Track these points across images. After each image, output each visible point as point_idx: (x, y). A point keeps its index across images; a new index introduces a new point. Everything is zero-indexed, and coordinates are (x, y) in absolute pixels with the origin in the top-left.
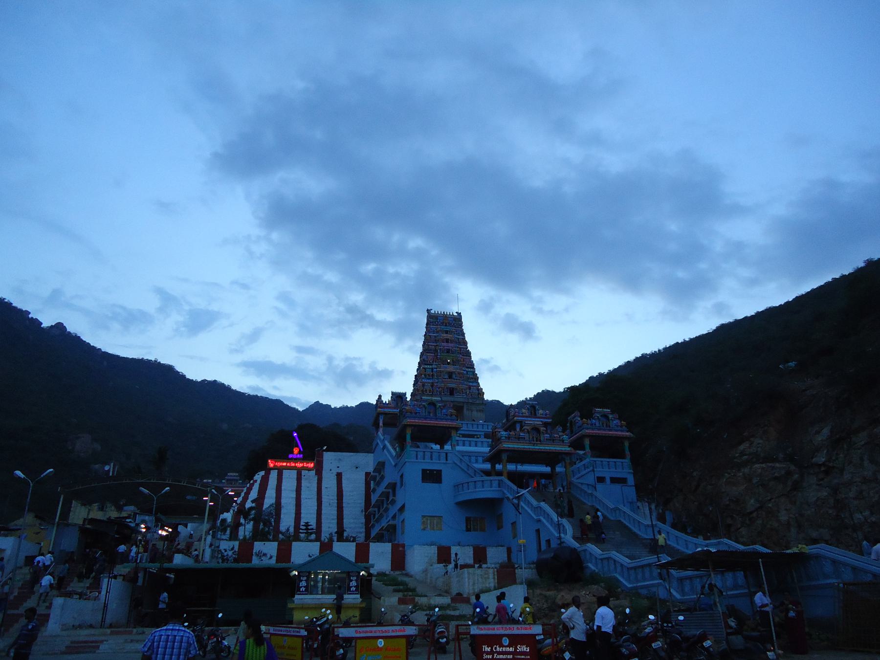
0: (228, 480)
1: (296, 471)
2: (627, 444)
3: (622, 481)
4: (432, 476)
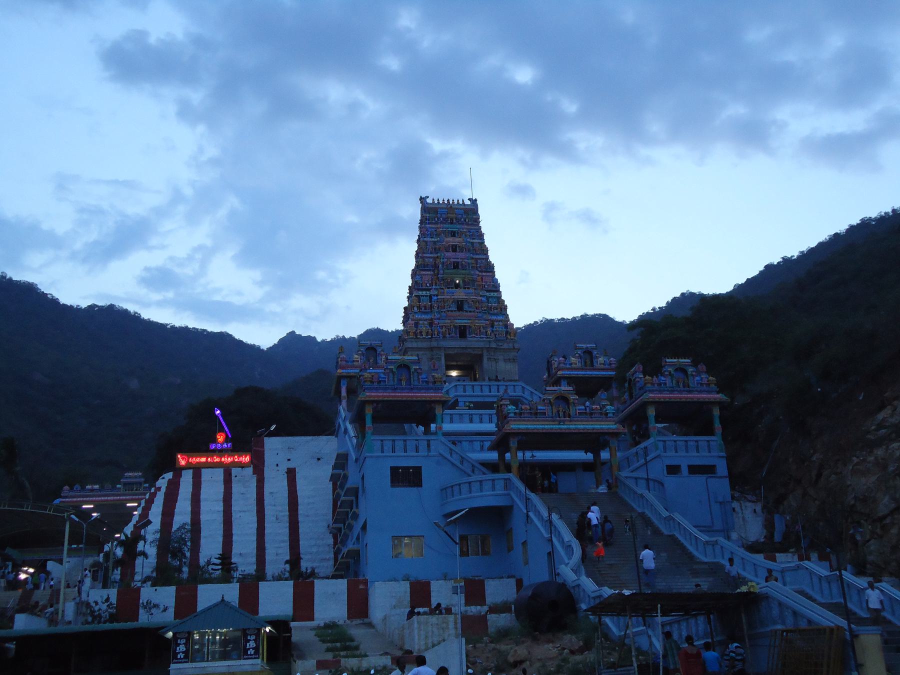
0: (125, 484)
1: (222, 470)
2: (716, 412)
3: (708, 470)
4: (405, 477)
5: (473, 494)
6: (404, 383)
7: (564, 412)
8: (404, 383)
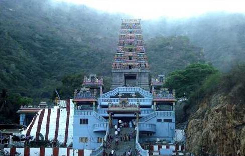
3: (170, 121)
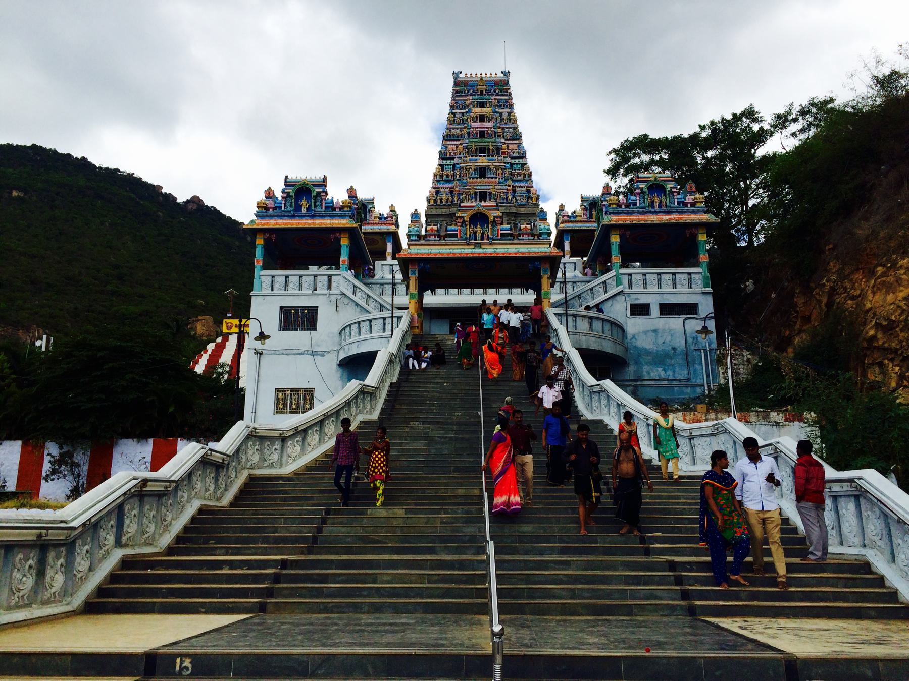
3: (689, 310)
5: (362, 337)
6: (304, 210)
7: (483, 234)
8: (304, 210)
